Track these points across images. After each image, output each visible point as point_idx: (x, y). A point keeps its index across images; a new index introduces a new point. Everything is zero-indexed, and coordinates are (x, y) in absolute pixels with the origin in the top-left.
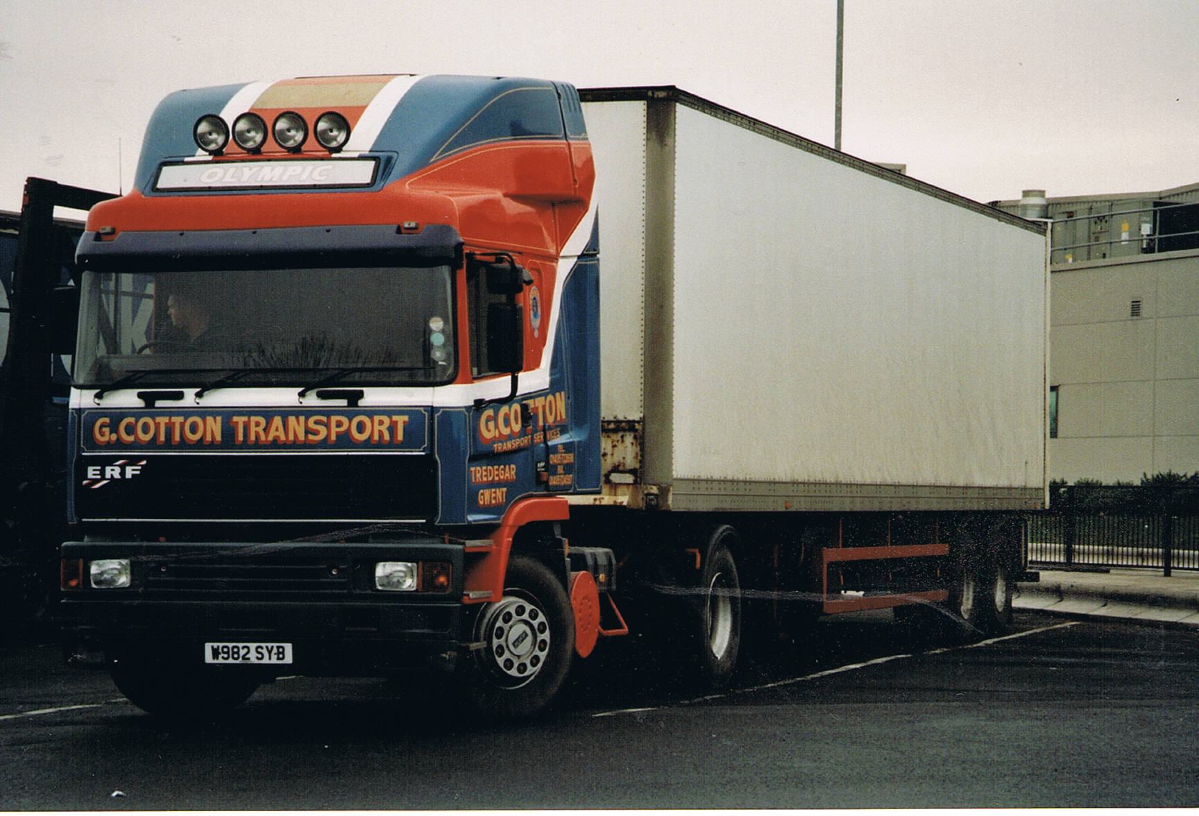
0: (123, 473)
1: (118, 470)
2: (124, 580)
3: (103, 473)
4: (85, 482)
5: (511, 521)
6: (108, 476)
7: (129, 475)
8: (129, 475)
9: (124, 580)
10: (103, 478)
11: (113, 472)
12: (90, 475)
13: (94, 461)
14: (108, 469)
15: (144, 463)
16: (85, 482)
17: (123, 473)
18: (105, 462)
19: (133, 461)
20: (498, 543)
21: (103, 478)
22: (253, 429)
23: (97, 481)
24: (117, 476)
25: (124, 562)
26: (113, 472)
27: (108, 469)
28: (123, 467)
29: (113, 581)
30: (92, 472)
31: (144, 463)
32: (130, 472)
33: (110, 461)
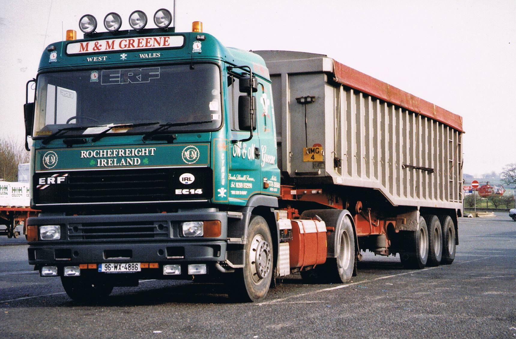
0: (56, 181)
1: (54, 179)
2: (57, 236)
4: (38, 186)
5: (250, 205)
6: (49, 183)
7: (59, 182)
8: (59, 182)
9: (57, 236)
10: (47, 184)
11: (51, 180)
12: (40, 183)
14: (49, 179)
15: (66, 175)
16: (38, 186)
17: (56, 181)
19: (61, 174)
20: (245, 215)
21: (47, 184)
22: (120, 153)
23: (43, 185)
24: (53, 182)
25: (57, 226)
26: (51, 180)
27: (49, 179)
28: (56, 178)
29: (52, 236)
30: (41, 181)
31: (66, 175)
33: (50, 175)
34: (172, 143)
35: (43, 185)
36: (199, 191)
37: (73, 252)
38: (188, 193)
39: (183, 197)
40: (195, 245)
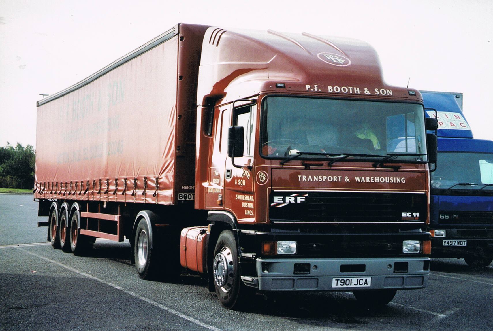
0: (296, 200)
3: (284, 200)
4: (272, 204)
10: (284, 202)
13: (279, 194)
15: (307, 195)
16: (272, 204)
17: (296, 200)
18: (285, 195)
19: (301, 194)
23: (281, 204)
24: (292, 201)
26: (290, 199)
30: (277, 199)
31: (307, 195)
32: (299, 200)
33: (289, 194)
34: (398, 171)
35: (281, 204)
36: (418, 214)
37: (312, 266)
38: (410, 216)
39: (407, 219)
40: (418, 261)
